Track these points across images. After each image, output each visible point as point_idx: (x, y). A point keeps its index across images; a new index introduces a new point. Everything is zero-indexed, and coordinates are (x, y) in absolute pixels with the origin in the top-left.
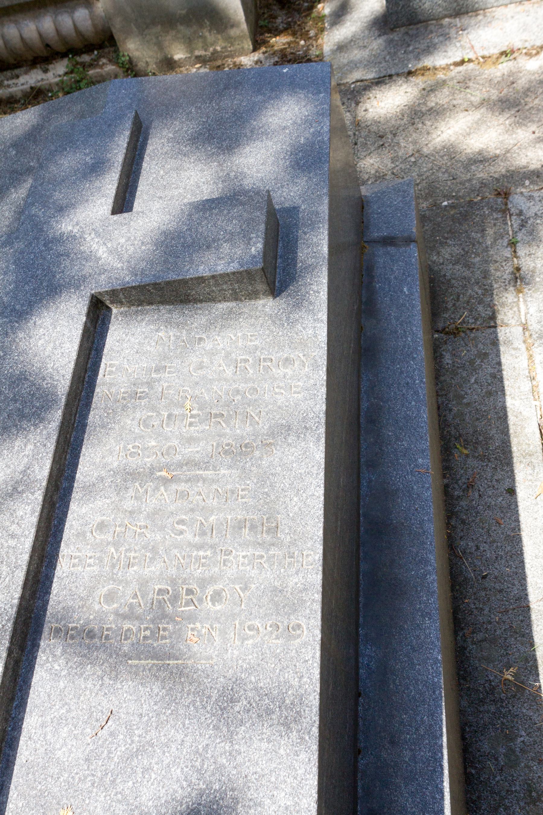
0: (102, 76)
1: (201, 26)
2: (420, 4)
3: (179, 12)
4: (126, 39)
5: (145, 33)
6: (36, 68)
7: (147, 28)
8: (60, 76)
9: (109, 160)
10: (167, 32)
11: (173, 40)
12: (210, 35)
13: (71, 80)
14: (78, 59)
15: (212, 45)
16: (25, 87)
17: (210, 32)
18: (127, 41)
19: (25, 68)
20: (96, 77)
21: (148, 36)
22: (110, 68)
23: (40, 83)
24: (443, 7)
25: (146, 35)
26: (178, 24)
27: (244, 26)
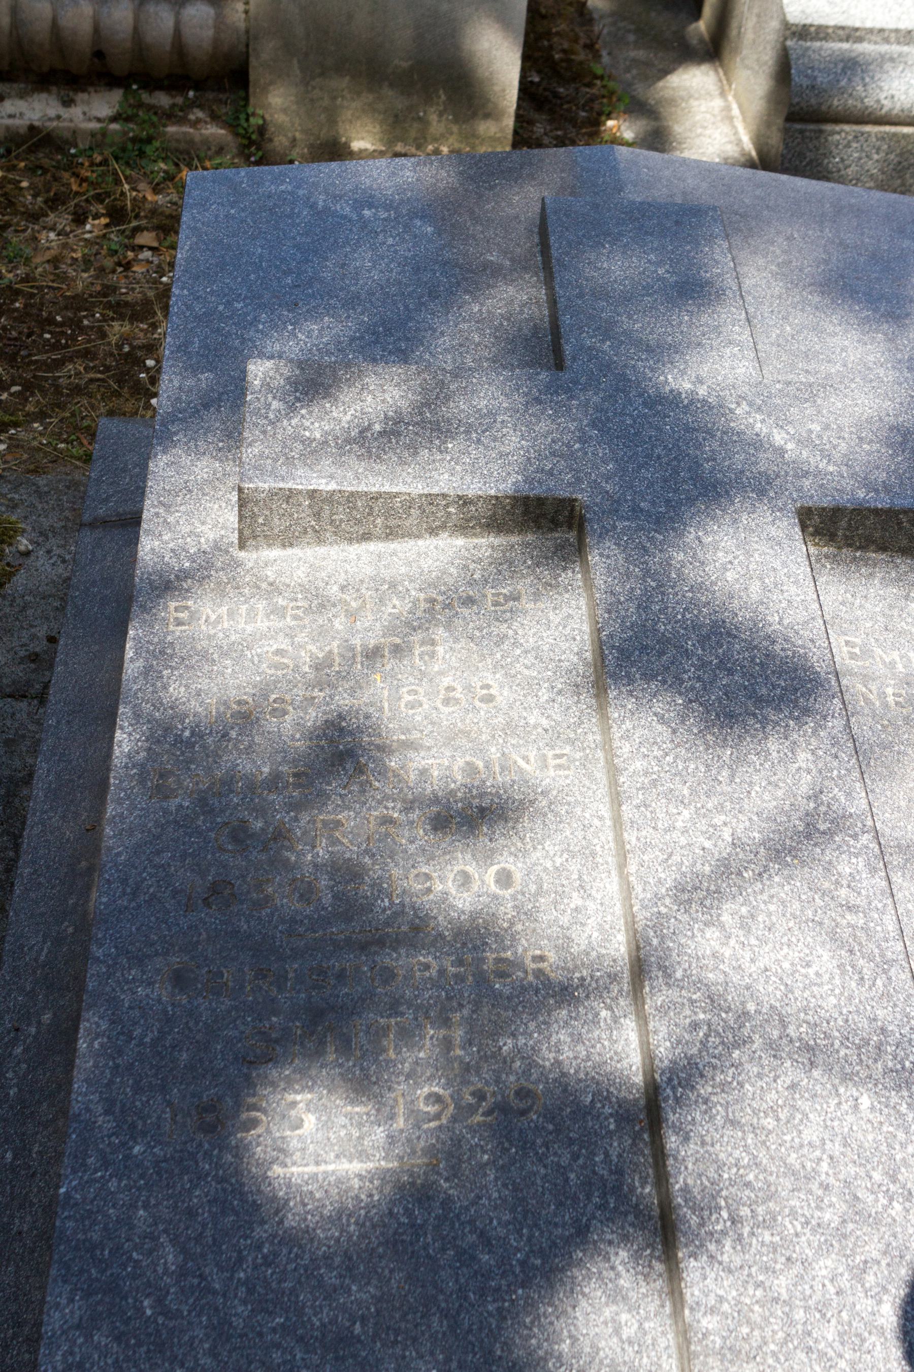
0: (191, 142)
1: (428, 99)
2: (841, 166)
3: (396, 62)
4: (271, 83)
5: (313, 83)
6: (49, 91)
7: (322, 74)
8: (99, 120)
9: (708, 283)
10: (359, 94)
11: (363, 111)
12: (439, 121)
13: (125, 133)
14: (145, 97)
15: (436, 140)
16: (17, 122)
17: (441, 115)
18: (271, 88)
19: (22, 86)
20: (178, 141)
21: (316, 91)
22: (214, 131)
23: (55, 124)
24: (877, 180)
25: (314, 88)
26: (387, 83)
27: (509, 122)
